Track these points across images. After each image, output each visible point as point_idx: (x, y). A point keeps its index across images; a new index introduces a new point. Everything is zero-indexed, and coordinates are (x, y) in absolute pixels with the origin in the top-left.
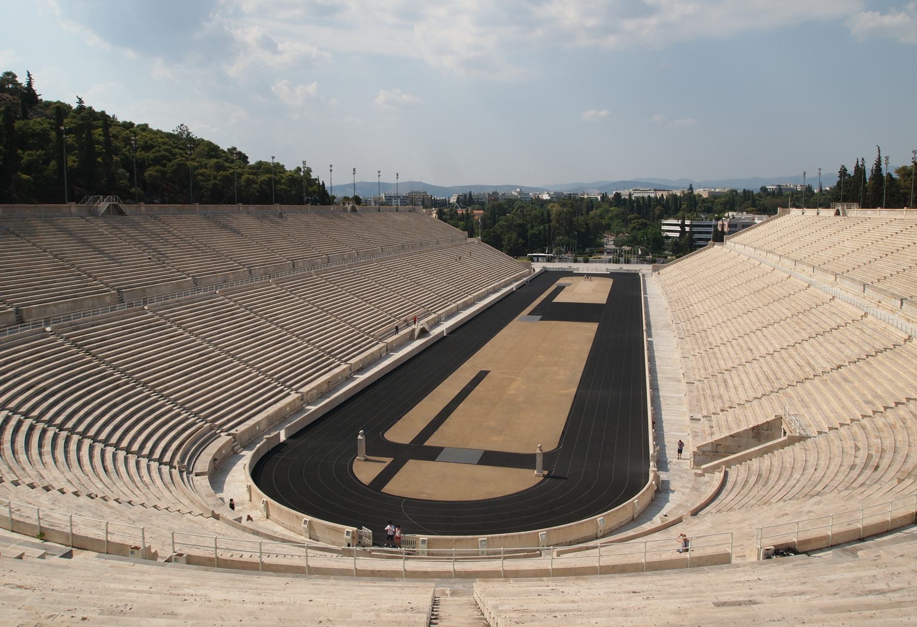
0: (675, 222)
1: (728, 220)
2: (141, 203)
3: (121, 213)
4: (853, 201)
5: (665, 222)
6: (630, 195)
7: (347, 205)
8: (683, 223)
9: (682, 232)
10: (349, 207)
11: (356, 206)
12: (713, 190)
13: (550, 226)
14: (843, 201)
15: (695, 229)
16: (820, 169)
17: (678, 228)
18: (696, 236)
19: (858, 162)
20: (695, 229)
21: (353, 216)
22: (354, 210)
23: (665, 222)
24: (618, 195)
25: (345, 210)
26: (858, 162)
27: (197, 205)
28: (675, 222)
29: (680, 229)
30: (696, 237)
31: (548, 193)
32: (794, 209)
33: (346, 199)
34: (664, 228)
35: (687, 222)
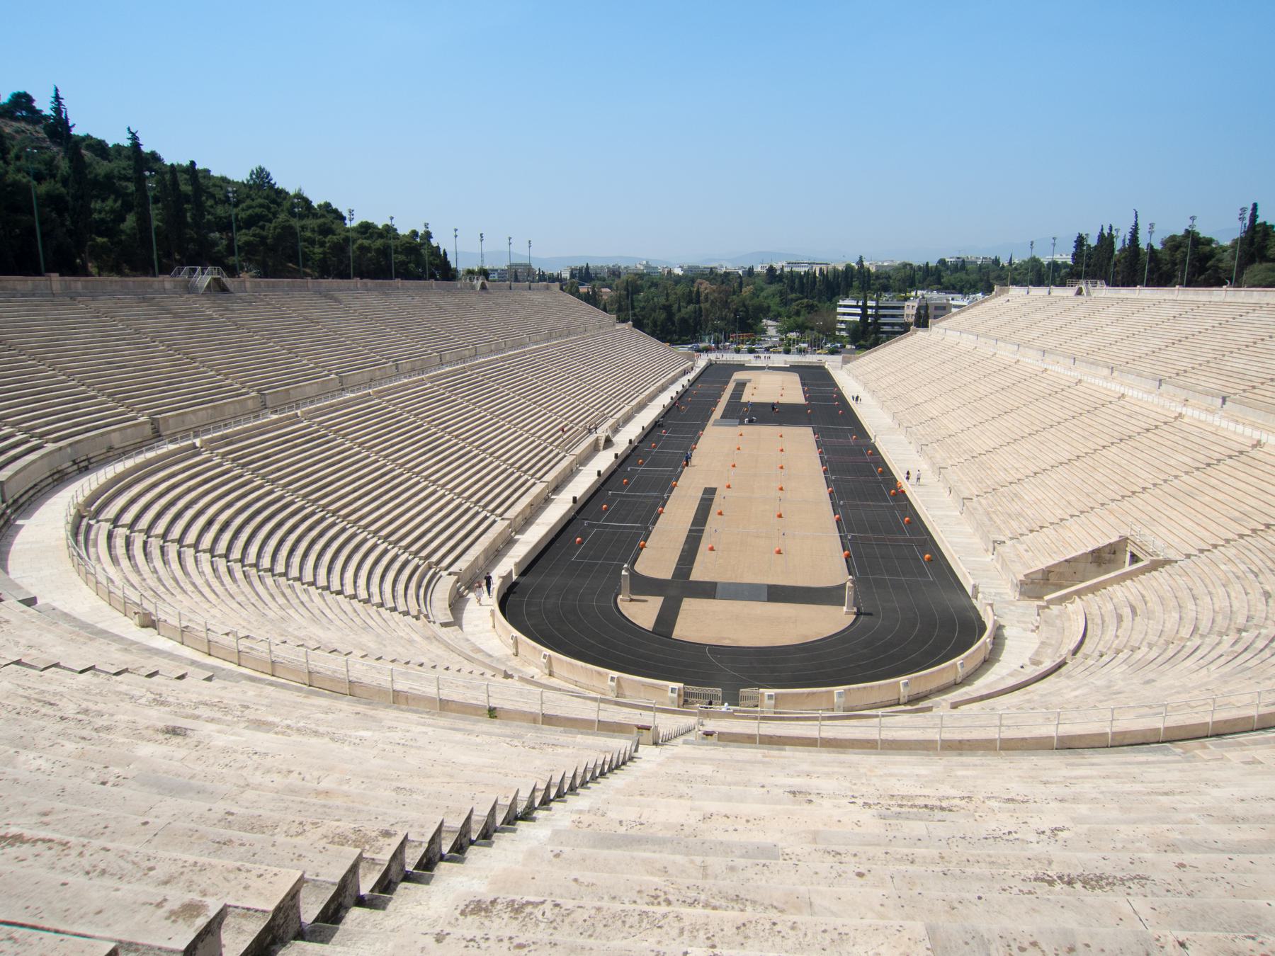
0: (854, 303)
1: (918, 300)
2: (52, 275)
3: (224, 289)
4: (1101, 278)
5: (841, 303)
6: (782, 269)
7: (475, 282)
8: (865, 303)
9: (864, 316)
10: (478, 283)
12: (880, 263)
13: (700, 308)
14: (1085, 278)
15: (882, 312)
16: (1054, 239)
17: (859, 311)
20: (882, 312)
21: (483, 293)
22: (483, 287)
23: (841, 303)
24: (771, 270)
25: (473, 288)
27: (55, 277)
28: (854, 303)
31: (680, 267)
32: (1014, 287)
33: (470, 272)
35: (870, 303)
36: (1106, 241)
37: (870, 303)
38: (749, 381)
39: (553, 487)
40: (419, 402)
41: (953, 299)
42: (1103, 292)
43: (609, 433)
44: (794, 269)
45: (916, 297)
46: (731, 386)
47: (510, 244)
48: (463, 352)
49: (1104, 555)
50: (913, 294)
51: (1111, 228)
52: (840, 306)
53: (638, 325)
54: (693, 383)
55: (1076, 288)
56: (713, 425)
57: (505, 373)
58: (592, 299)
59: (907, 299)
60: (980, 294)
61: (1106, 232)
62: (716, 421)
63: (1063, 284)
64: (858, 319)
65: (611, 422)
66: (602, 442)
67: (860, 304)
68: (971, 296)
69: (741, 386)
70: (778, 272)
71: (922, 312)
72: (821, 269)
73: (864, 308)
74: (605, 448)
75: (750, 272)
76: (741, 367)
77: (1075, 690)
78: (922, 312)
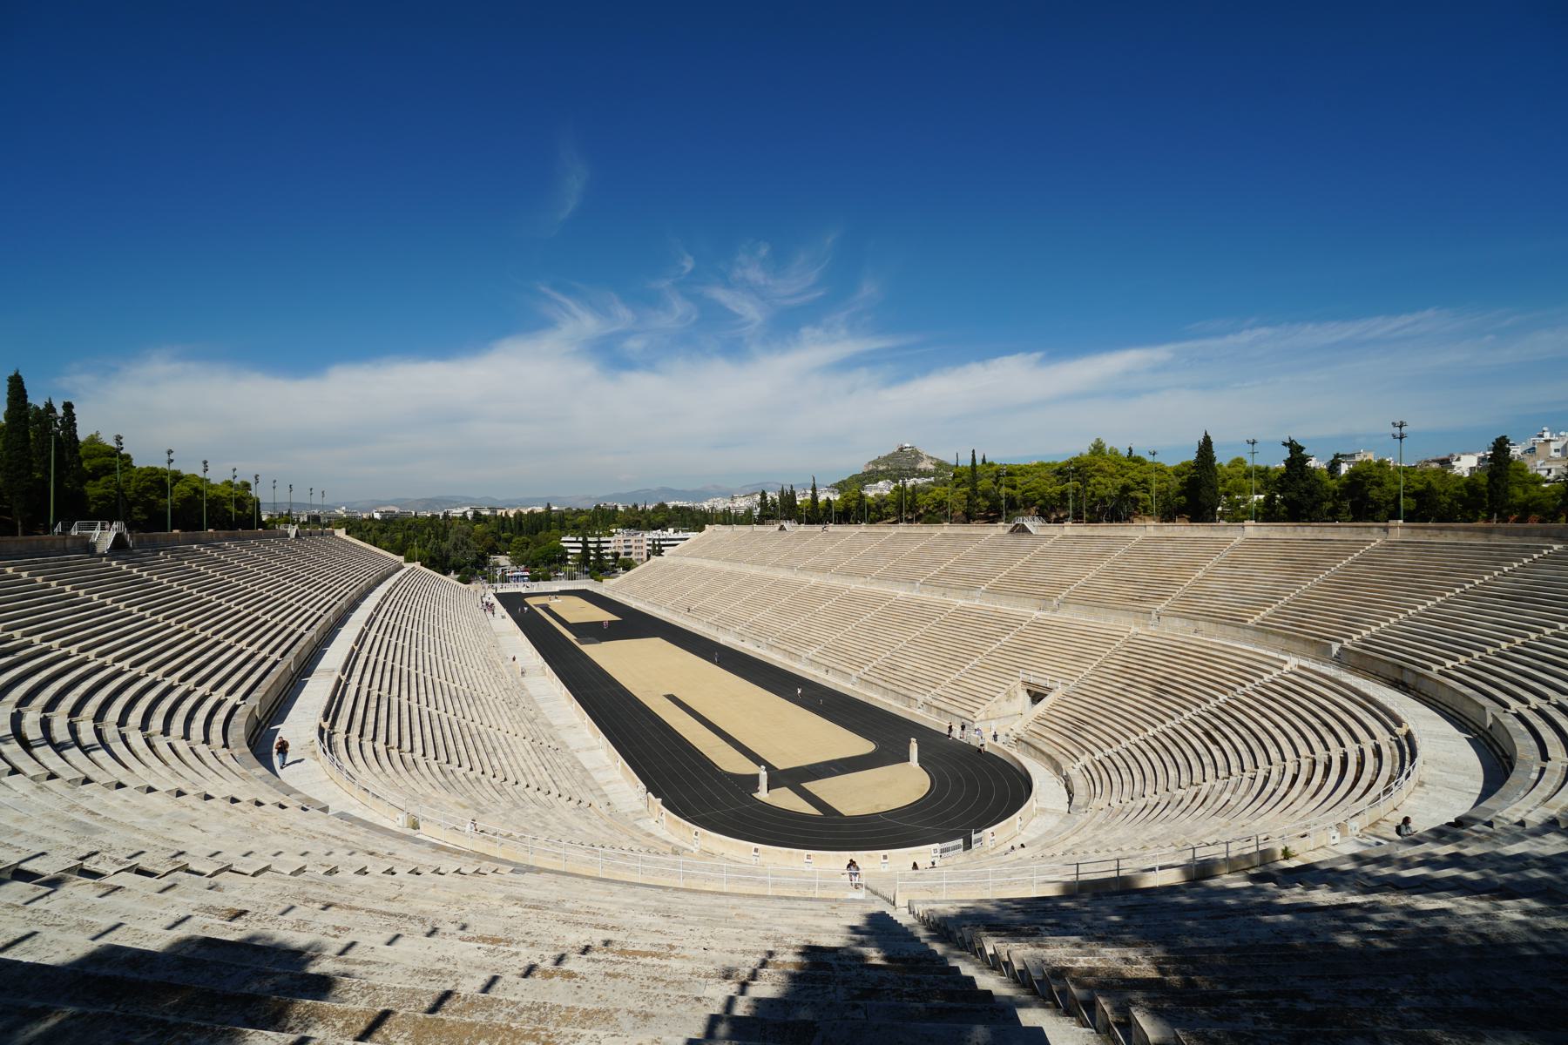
0: (574, 539)
5: (563, 539)
8: (585, 539)
9: (585, 549)
17: (580, 545)
18: (605, 551)
20: (603, 545)
23: (563, 539)
28: (574, 539)
34: (565, 545)
35: (589, 539)
37: (589, 539)
52: (565, 542)
64: (579, 551)
67: (580, 539)
73: (585, 542)
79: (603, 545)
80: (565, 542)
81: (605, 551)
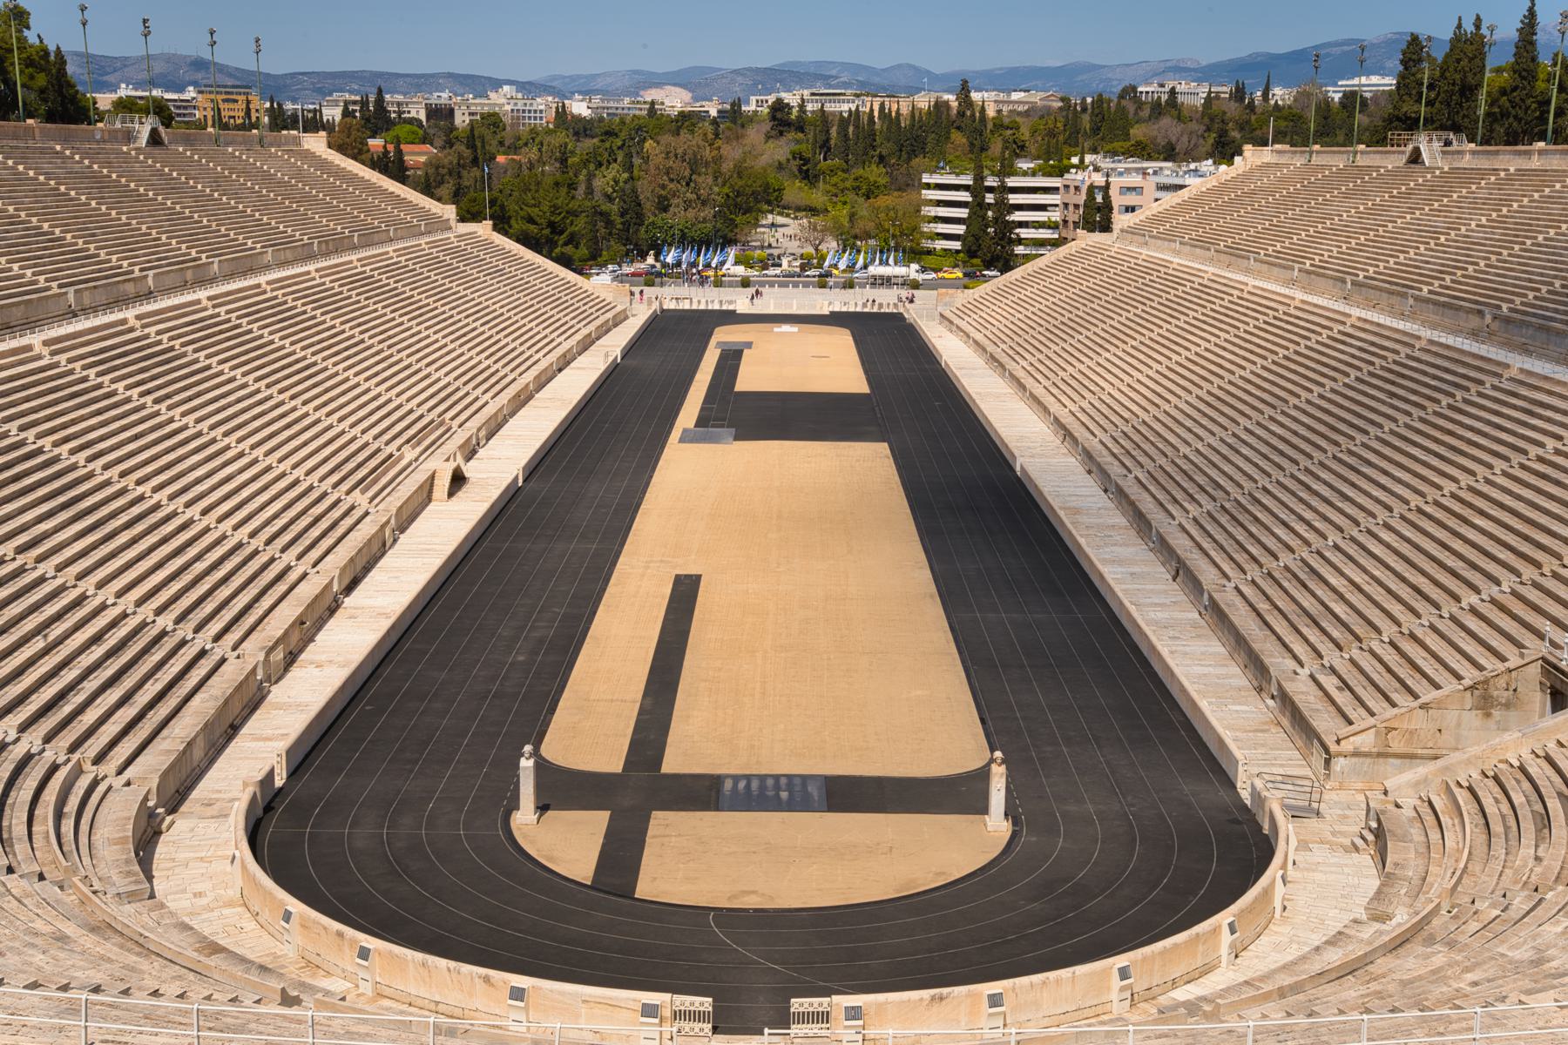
8: (979, 178)
9: (978, 206)
10: (144, 129)
11: (162, 129)
17: (965, 196)
18: (1018, 216)
19: (1459, 26)
20: (1014, 199)
21: (157, 151)
22: (155, 139)
26: (1459, 26)
29: (970, 199)
30: (1017, 219)
36: (1468, 47)
38: (749, 345)
39: (346, 581)
40: (27, 399)
41: (1155, 173)
42: (1468, 154)
43: (460, 460)
44: (829, 107)
45: (1081, 166)
46: (710, 359)
47: (213, 44)
48: (121, 287)
49: (1495, 693)
50: (1075, 160)
51: (1478, 23)
52: (928, 186)
53: (501, 226)
54: (630, 350)
55: (1410, 147)
56: (682, 440)
57: (221, 332)
58: (393, 167)
59: (1061, 171)
60: (1210, 162)
61: (1469, 27)
62: (685, 431)
63: (1378, 139)
64: (963, 213)
65: (460, 437)
66: (443, 483)
68: (1192, 166)
69: (731, 359)
70: (795, 111)
71: (1099, 199)
72: (882, 106)
74: (451, 494)
75: (734, 115)
76: (730, 317)
77: (1467, 970)
78: (1099, 199)
79: (1014, 199)
80: (928, 186)
81: (1018, 216)
